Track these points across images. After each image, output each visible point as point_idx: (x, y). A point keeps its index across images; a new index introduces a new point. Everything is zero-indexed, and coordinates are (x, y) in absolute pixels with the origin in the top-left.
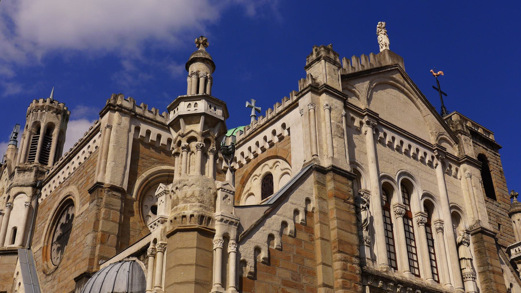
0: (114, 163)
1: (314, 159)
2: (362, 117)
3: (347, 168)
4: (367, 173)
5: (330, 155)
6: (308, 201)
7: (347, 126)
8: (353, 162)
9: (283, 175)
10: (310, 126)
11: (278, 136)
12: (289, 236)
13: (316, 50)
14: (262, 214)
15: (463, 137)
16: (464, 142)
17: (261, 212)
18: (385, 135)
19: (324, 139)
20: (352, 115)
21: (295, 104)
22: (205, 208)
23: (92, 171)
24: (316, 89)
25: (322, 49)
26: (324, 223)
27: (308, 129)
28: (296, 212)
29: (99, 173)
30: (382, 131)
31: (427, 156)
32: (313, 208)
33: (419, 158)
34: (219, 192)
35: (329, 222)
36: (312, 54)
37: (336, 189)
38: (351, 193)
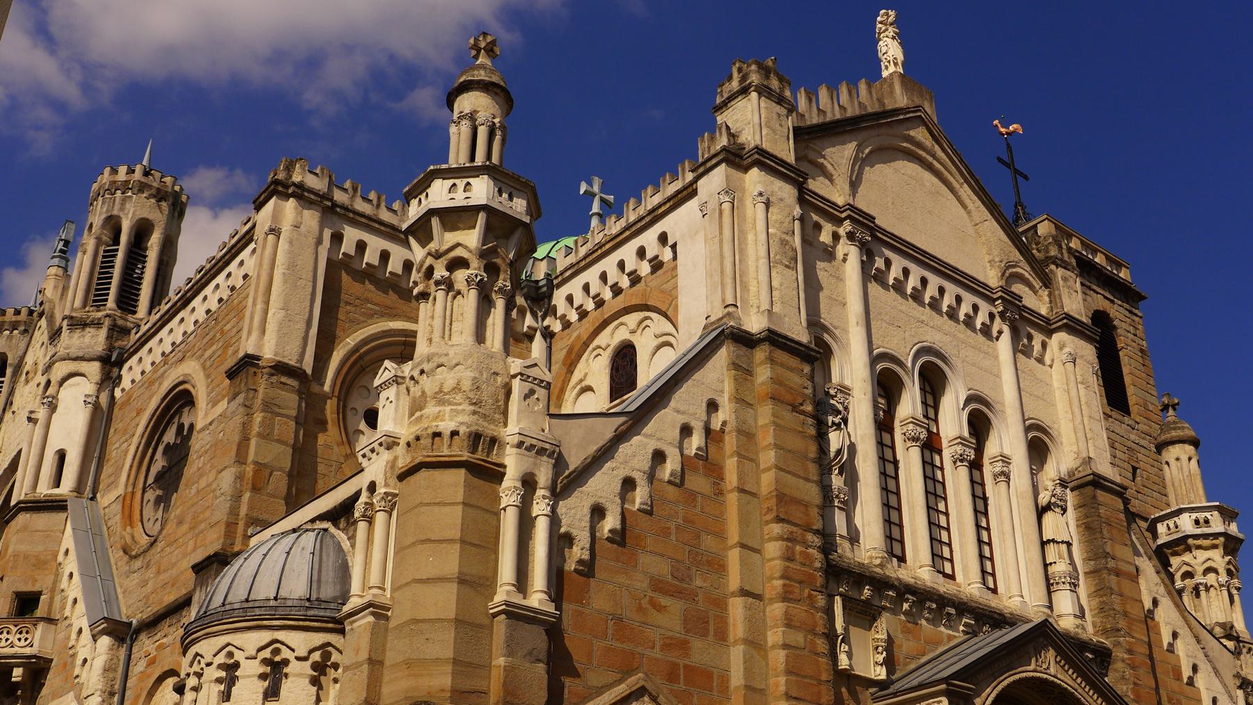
0: (283, 313)
1: (729, 314)
2: (839, 222)
3: (803, 337)
4: (845, 347)
5: (765, 306)
6: (712, 406)
7: (805, 241)
8: (815, 323)
9: (659, 347)
10: (721, 241)
11: (650, 261)
12: (669, 482)
13: (740, 70)
14: (609, 434)
15: (1060, 272)
16: (1061, 282)
17: (607, 429)
18: (888, 263)
19: (752, 270)
20: (815, 218)
21: (690, 190)
22: (485, 416)
23: (235, 330)
24: (737, 157)
25: (753, 67)
26: (746, 456)
27: (717, 247)
28: (686, 431)
29: (249, 333)
30: (882, 255)
31: (980, 313)
32: (724, 423)
33: (962, 317)
34: (516, 383)
35: (757, 454)
36: (730, 78)
37: (775, 380)
38: (809, 391)
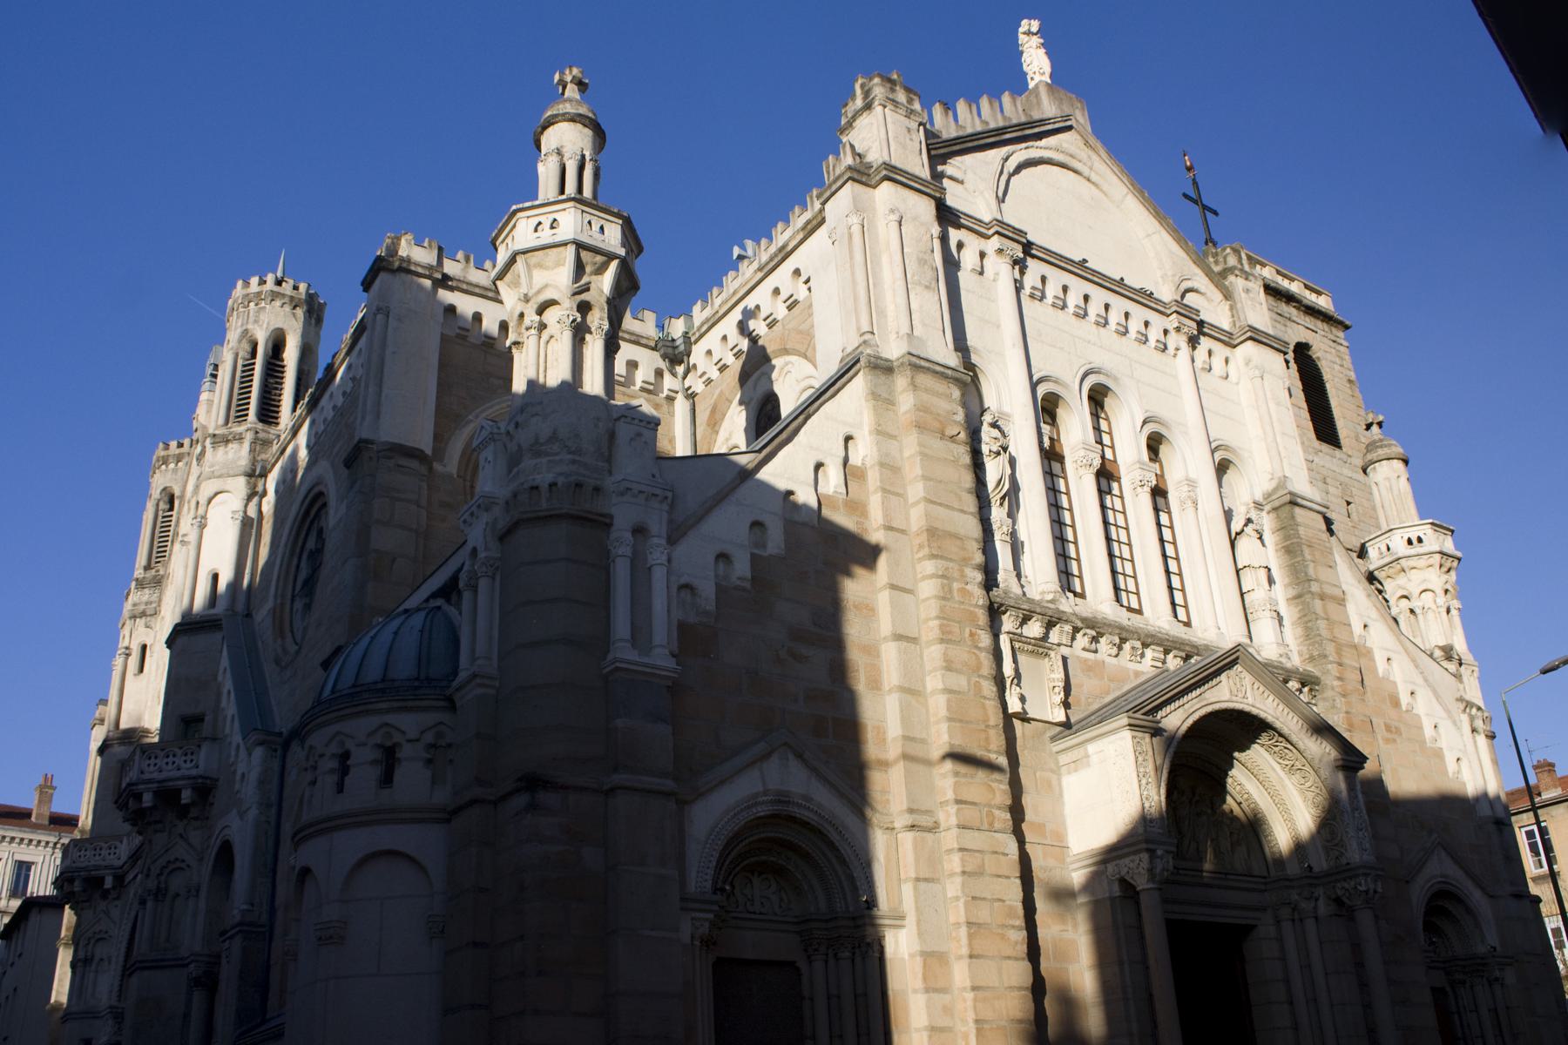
37: (921, 408)
